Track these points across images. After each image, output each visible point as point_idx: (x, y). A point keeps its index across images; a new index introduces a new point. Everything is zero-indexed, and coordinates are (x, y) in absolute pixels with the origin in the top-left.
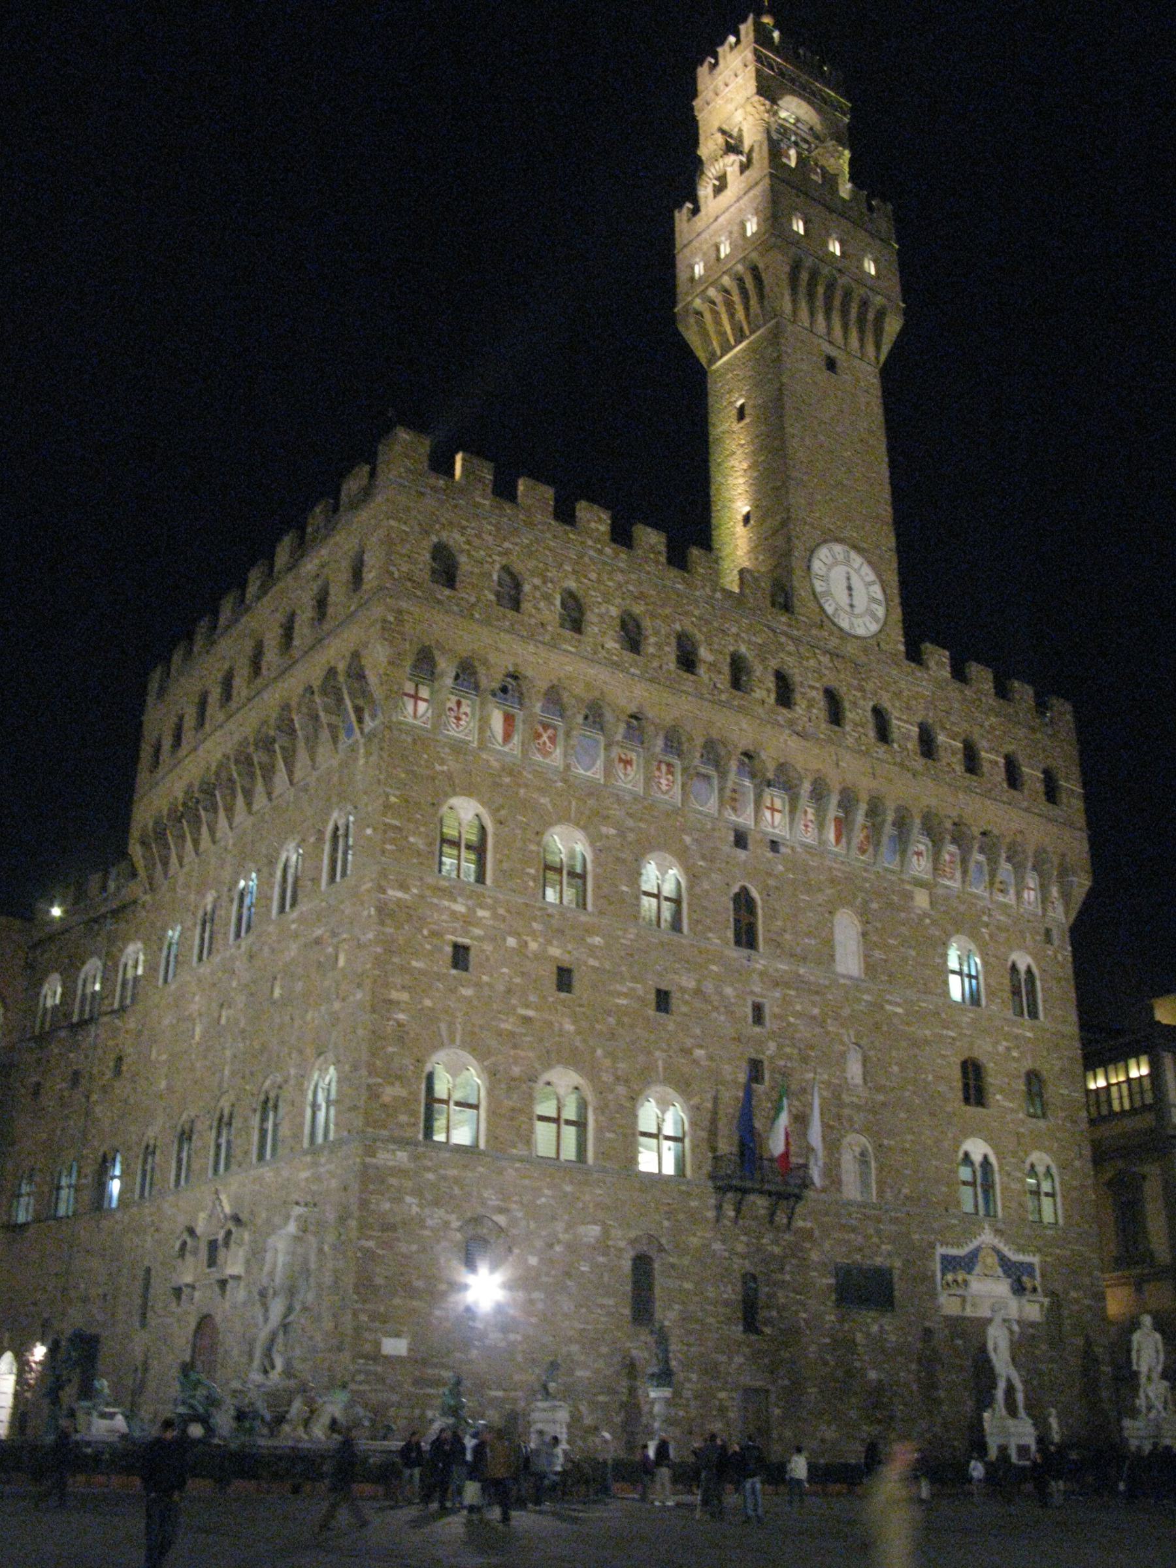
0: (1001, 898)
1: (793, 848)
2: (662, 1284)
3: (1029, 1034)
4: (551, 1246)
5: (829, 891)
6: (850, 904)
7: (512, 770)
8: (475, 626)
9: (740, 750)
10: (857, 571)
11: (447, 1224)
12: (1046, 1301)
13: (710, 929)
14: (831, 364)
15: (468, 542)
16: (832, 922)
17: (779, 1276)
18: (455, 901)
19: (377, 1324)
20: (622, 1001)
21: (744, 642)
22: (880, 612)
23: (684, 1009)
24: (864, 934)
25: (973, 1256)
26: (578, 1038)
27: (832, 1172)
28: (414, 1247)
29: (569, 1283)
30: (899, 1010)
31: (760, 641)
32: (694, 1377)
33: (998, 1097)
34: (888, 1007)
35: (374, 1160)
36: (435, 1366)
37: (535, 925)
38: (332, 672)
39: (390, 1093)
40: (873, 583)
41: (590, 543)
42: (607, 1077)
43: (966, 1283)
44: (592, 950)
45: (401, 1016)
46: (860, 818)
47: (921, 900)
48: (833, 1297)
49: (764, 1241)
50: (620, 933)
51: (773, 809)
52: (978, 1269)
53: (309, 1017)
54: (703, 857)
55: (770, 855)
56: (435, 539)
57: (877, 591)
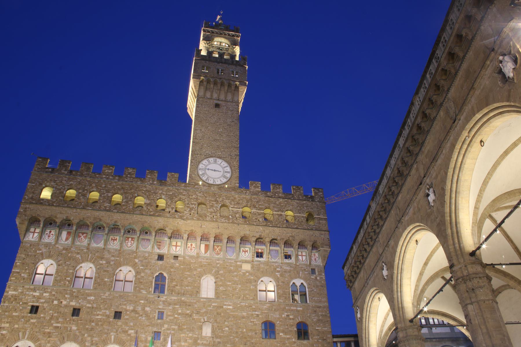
0: (287, 261)
1: (184, 257)
3: (301, 309)
6: (210, 272)
7: (67, 249)
8: (54, 208)
9: (157, 229)
10: (220, 165)
13: (143, 289)
15: (57, 184)
16: (200, 281)
18: (36, 292)
20: (100, 317)
21: (164, 194)
22: (229, 175)
23: (126, 317)
24: (215, 282)
26: (77, 331)
30: (231, 307)
31: (171, 193)
33: (281, 334)
34: (224, 307)
37: (66, 296)
40: (227, 166)
41: (104, 176)
44: (89, 302)
47: (247, 267)
50: (102, 294)
51: (176, 246)
54: (143, 266)
57: (228, 169)
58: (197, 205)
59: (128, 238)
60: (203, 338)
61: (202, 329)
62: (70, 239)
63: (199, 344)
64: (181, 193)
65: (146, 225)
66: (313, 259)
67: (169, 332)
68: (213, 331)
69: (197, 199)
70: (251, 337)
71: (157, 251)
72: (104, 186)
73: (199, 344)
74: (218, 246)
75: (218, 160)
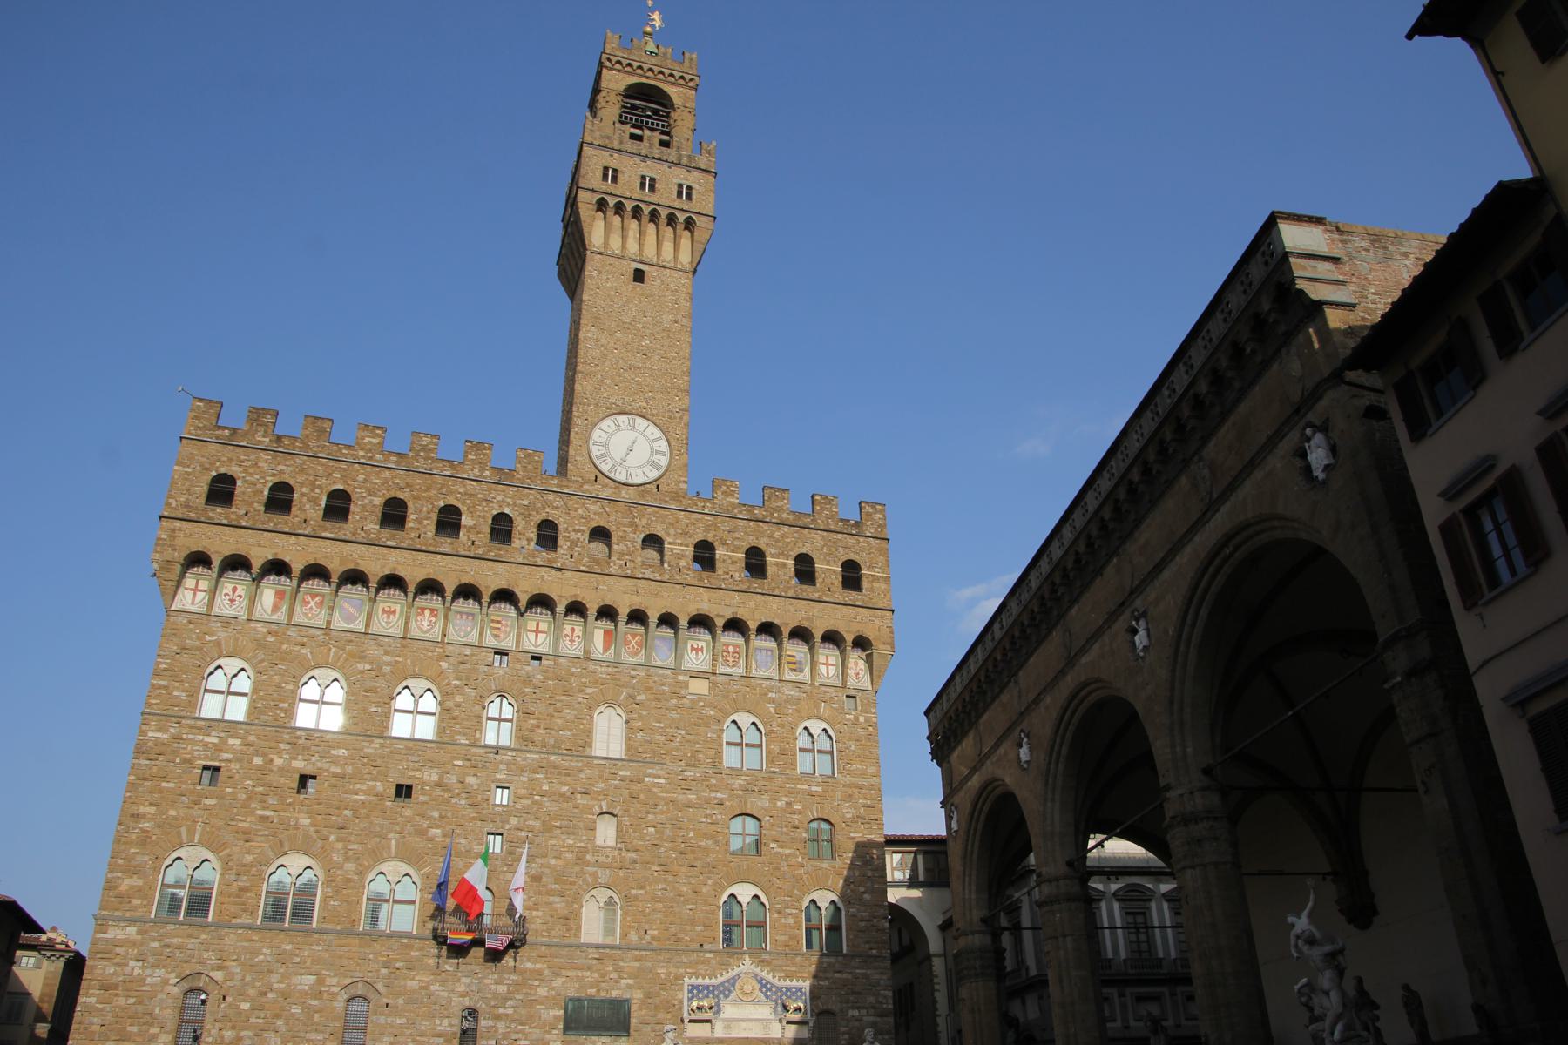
5: (590, 691)
11: (166, 982)
13: (459, 733)
14: (639, 276)
15: (245, 471)
17: (501, 1010)
23: (422, 798)
27: (571, 920)
28: (132, 1000)
29: (279, 1023)
41: (362, 453)
43: (716, 1009)
44: (334, 761)
47: (699, 687)
48: (561, 1026)
51: (537, 632)
52: (733, 995)
56: (214, 474)
57: (663, 445)
58: (587, 535)
59: (423, 609)
60: (597, 850)
61: (594, 829)
62: (284, 609)
63: (588, 863)
64: (548, 503)
65: (466, 580)
66: (851, 672)
67: (523, 834)
68: (620, 833)
69: (587, 518)
70: (706, 850)
71: (490, 641)
72: (361, 478)
73: (588, 863)
74: (634, 636)
75: (639, 420)
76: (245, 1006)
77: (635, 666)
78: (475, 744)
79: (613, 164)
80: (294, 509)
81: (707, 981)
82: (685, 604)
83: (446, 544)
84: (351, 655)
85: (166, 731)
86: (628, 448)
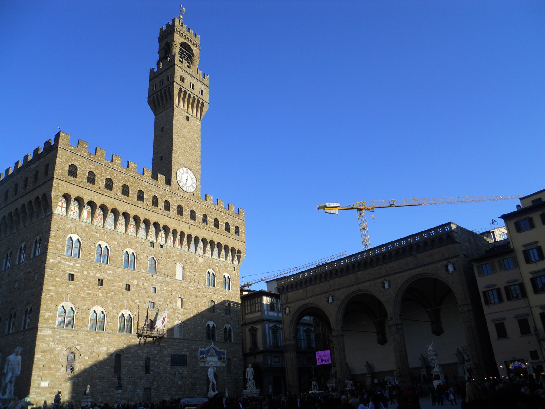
2: (124, 362)
4: (92, 354)
5: (175, 258)
11: (62, 350)
12: (227, 361)
14: (188, 119)
15: (80, 165)
19: (40, 378)
22: (195, 186)
23: (133, 290)
25: (209, 350)
28: (52, 356)
32: (131, 386)
35: (42, 333)
36: (56, 388)
38: (38, 198)
39: (47, 314)
41: (115, 166)
42: (110, 308)
43: (206, 358)
45: (52, 294)
46: (186, 239)
47: (200, 260)
49: (152, 349)
51: (162, 237)
53: (25, 293)
55: (160, 249)
60: (177, 308)
63: (176, 313)
72: (115, 175)
76: (87, 358)
77: (186, 251)
78: (146, 273)
79: (183, 76)
80: (96, 183)
81: (204, 350)
82: (202, 234)
83: (140, 203)
84: (111, 238)
85: (56, 259)
86: (186, 178)
